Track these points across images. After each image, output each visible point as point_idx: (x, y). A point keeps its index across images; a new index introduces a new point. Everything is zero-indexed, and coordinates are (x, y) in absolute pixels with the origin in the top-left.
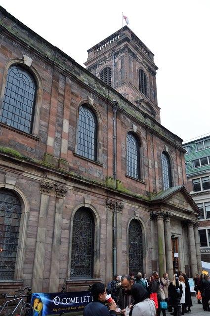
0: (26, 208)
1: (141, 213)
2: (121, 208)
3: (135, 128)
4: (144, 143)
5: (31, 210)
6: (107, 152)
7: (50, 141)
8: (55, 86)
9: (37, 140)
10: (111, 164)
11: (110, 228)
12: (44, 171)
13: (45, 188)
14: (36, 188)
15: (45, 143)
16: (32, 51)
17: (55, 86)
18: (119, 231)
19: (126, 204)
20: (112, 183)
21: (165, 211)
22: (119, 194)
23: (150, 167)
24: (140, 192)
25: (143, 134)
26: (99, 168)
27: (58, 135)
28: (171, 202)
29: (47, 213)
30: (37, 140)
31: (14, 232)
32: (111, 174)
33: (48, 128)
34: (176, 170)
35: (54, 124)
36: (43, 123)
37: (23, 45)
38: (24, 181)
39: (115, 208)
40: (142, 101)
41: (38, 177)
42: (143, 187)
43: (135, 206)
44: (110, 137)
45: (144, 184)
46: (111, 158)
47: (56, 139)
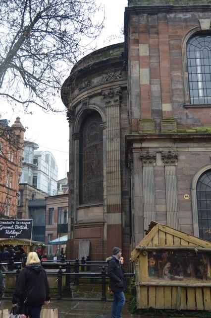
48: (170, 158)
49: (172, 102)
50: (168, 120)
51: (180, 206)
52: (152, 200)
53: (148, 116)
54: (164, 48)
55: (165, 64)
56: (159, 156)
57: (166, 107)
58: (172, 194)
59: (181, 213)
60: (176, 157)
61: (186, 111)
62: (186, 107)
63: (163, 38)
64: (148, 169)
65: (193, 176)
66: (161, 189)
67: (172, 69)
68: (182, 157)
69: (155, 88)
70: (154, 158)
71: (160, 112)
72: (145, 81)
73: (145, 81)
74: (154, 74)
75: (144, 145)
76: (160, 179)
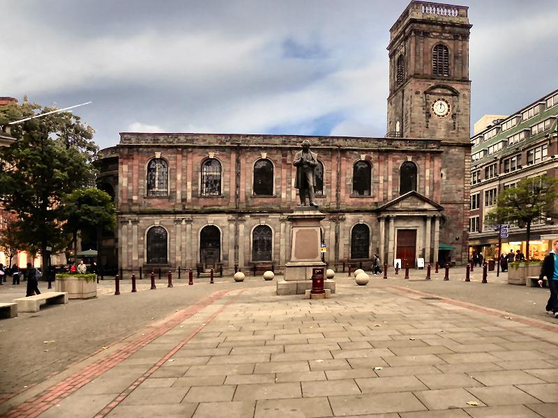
0: (273, 232)
1: (364, 219)
2: (343, 220)
3: (363, 157)
4: (376, 165)
5: (275, 232)
6: (331, 186)
7: (284, 195)
8: (284, 161)
9: (275, 197)
10: (334, 193)
11: (333, 233)
12: (281, 212)
13: (282, 221)
14: (278, 222)
15: (281, 197)
16: (265, 149)
17: (284, 161)
18: (341, 235)
19: (348, 216)
20: (334, 206)
21: (385, 215)
22: (342, 211)
23: (382, 182)
24: (367, 203)
25: (373, 156)
26: (322, 199)
27: (289, 190)
28: (396, 207)
29: (285, 232)
30: (275, 197)
31: (269, 243)
32: (334, 199)
33: (281, 188)
34: (422, 173)
35: (285, 184)
36: (278, 186)
37: (260, 148)
38: (270, 220)
39: (336, 221)
40: (433, 88)
41: (278, 216)
42: (371, 200)
43: (361, 215)
44: (334, 174)
45: (373, 197)
46: (334, 190)
47: (287, 192)
48: (135, 222)
49: (137, 194)
50: (136, 204)
51: (139, 242)
52: (126, 240)
53: (126, 202)
54: (136, 168)
55: (136, 176)
56: (130, 221)
57: (135, 198)
58: (135, 237)
59: (139, 245)
60: (138, 222)
61: (145, 200)
62: (145, 198)
63: (136, 162)
64: (125, 227)
65: (145, 230)
66: (130, 235)
67: (139, 178)
68: (141, 221)
69: (130, 188)
70: (128, 222)
71: (132, 200)
72: (125, 184)
73: (125, 184)
74: (130, 180)
75: (123, 216)
76: (130, 231)
